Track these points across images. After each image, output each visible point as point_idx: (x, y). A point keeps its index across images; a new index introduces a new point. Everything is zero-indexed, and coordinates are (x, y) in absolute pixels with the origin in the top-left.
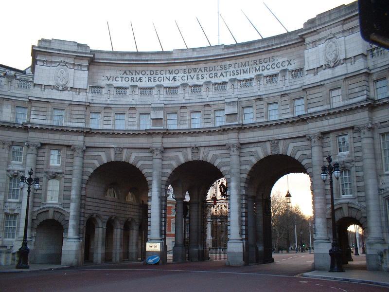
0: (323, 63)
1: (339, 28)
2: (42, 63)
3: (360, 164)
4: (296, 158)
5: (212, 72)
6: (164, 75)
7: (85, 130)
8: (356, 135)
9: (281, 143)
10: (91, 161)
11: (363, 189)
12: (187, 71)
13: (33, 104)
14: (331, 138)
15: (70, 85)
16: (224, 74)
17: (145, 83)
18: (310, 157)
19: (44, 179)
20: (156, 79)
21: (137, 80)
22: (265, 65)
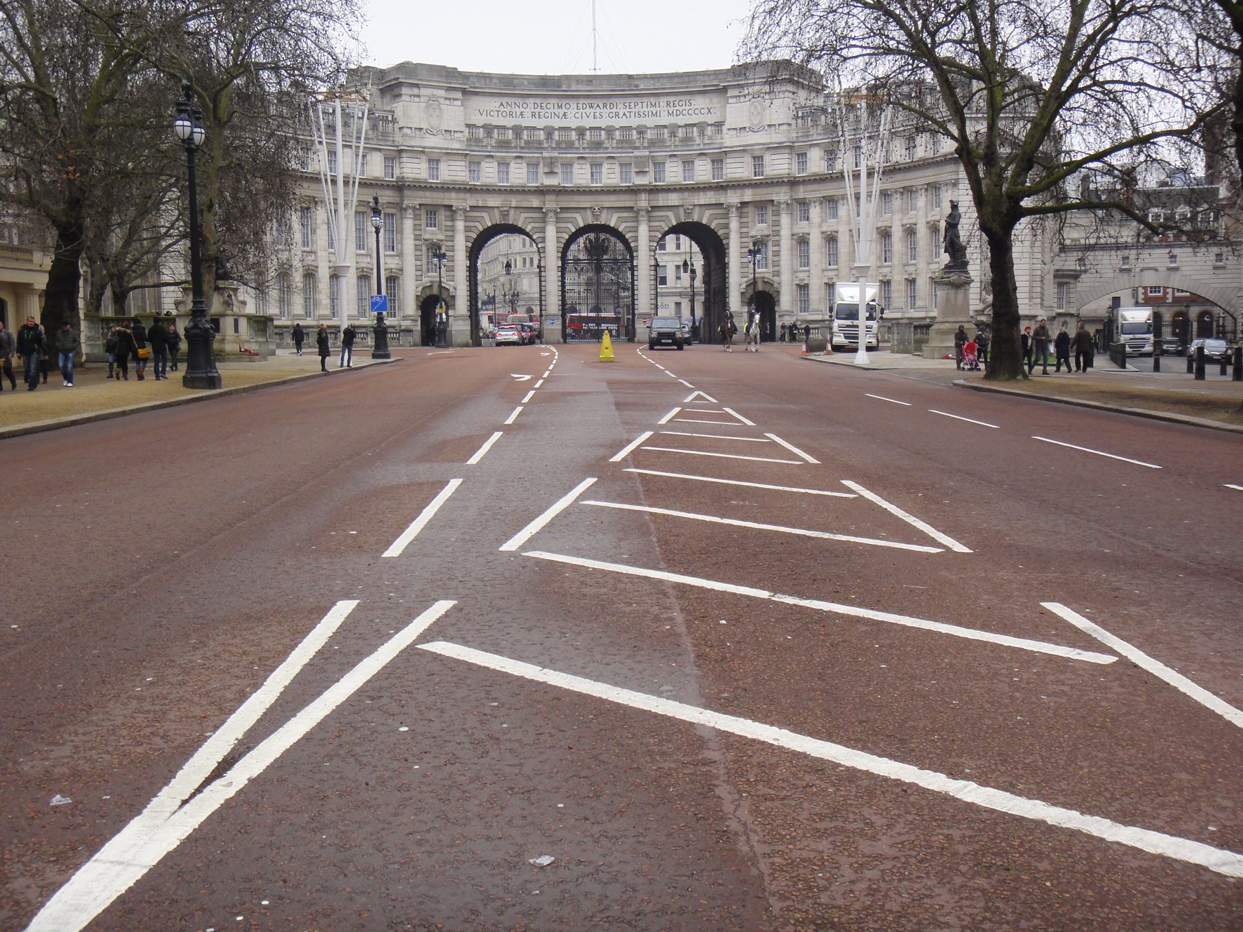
0: (747, 125)
1: (767, 88)
2: (408, 98)
3: (777, 238)
4: (712, 227)
5: (614, 110)
6: (552, 110)
7: (468, 187)
8: (775, 208)
9: (697, 209)
10: (472, 224)
11: (777, 264)
12: (580, 106)
13: (404, 155)
14: (750, 210)
15: (444, 127)
16: (628, 114)
17: (527, 122)
18: (727, 226)
19: (424, 248)
20: (542, 114)
21: (518, 114)
22: (681, 109)
